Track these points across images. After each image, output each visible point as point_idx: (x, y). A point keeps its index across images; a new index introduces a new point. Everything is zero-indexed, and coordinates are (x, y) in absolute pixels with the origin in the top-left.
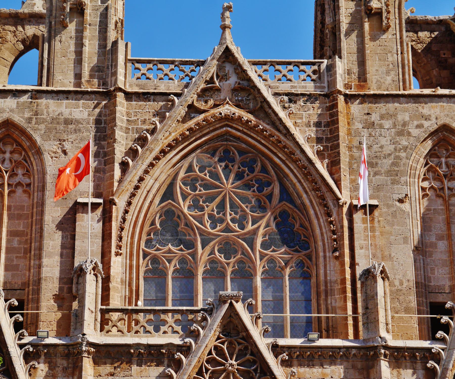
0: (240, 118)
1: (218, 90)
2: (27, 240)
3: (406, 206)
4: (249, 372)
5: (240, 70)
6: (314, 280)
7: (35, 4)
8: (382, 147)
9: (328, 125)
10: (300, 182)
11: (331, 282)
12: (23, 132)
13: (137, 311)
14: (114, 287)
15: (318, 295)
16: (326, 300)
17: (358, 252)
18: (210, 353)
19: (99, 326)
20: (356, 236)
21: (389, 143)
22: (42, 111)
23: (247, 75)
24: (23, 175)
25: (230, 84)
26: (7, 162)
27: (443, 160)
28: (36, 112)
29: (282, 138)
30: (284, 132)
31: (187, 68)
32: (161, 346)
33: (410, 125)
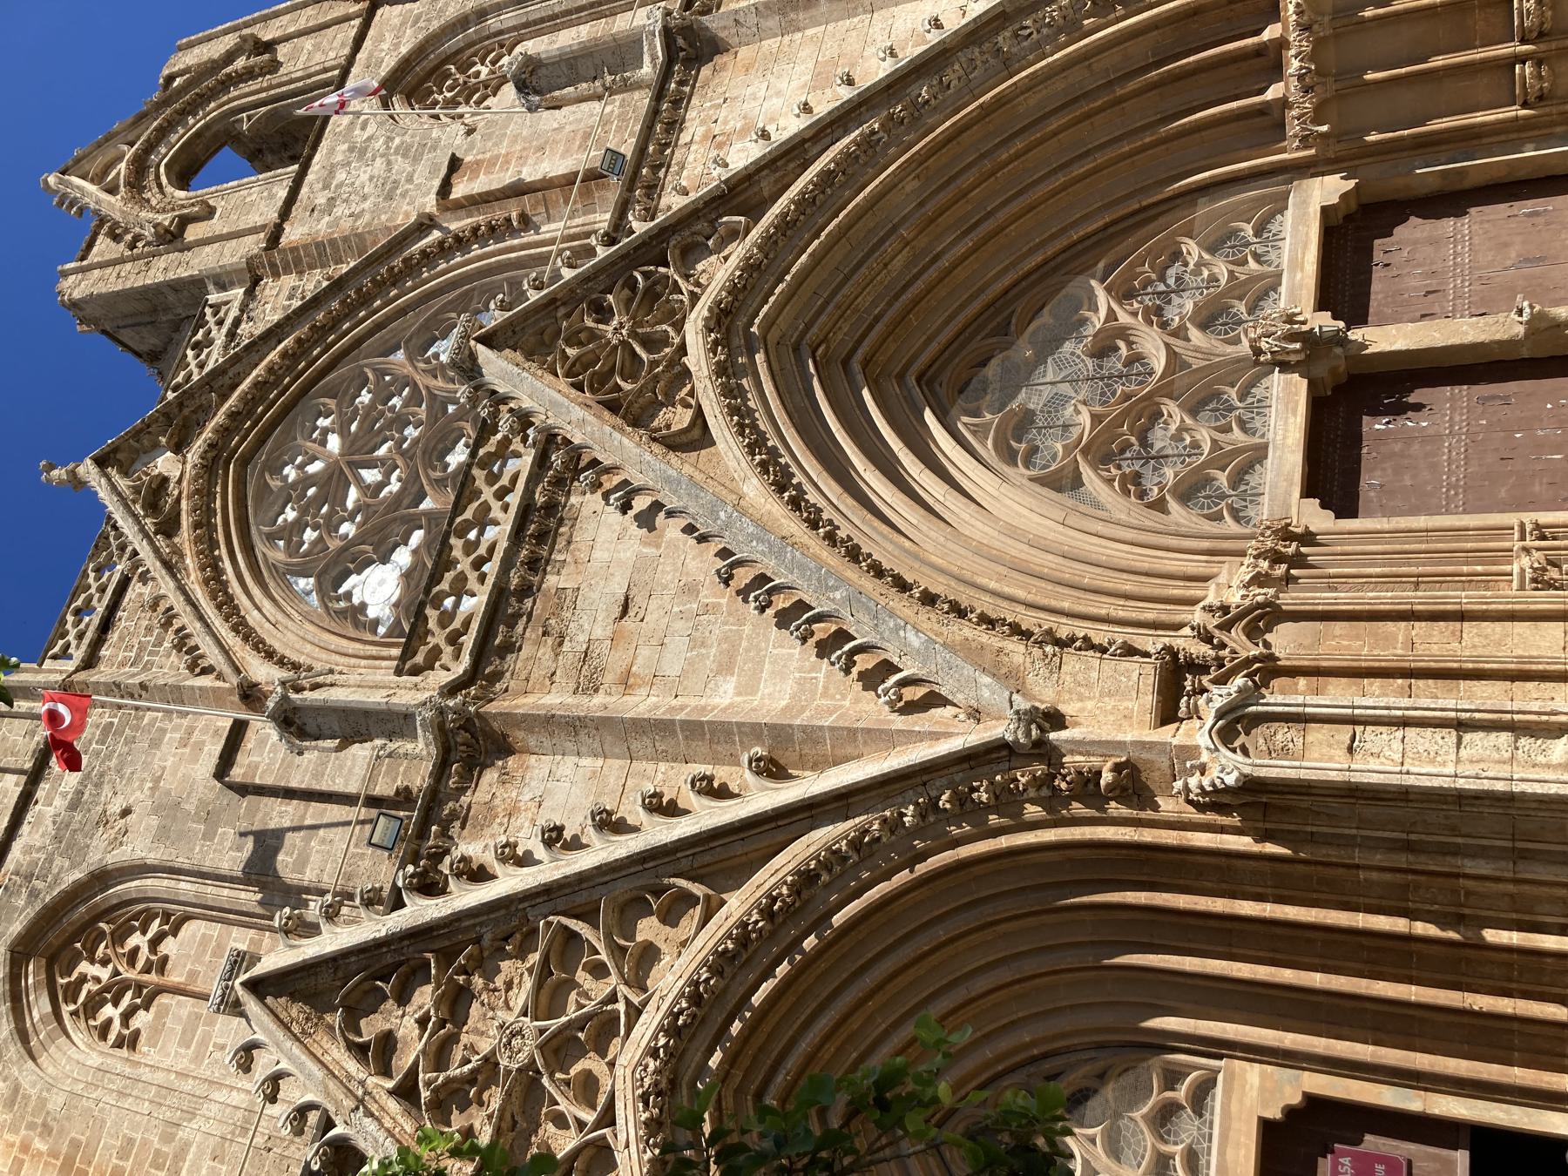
8: (371, 179)
28: (26, 878)
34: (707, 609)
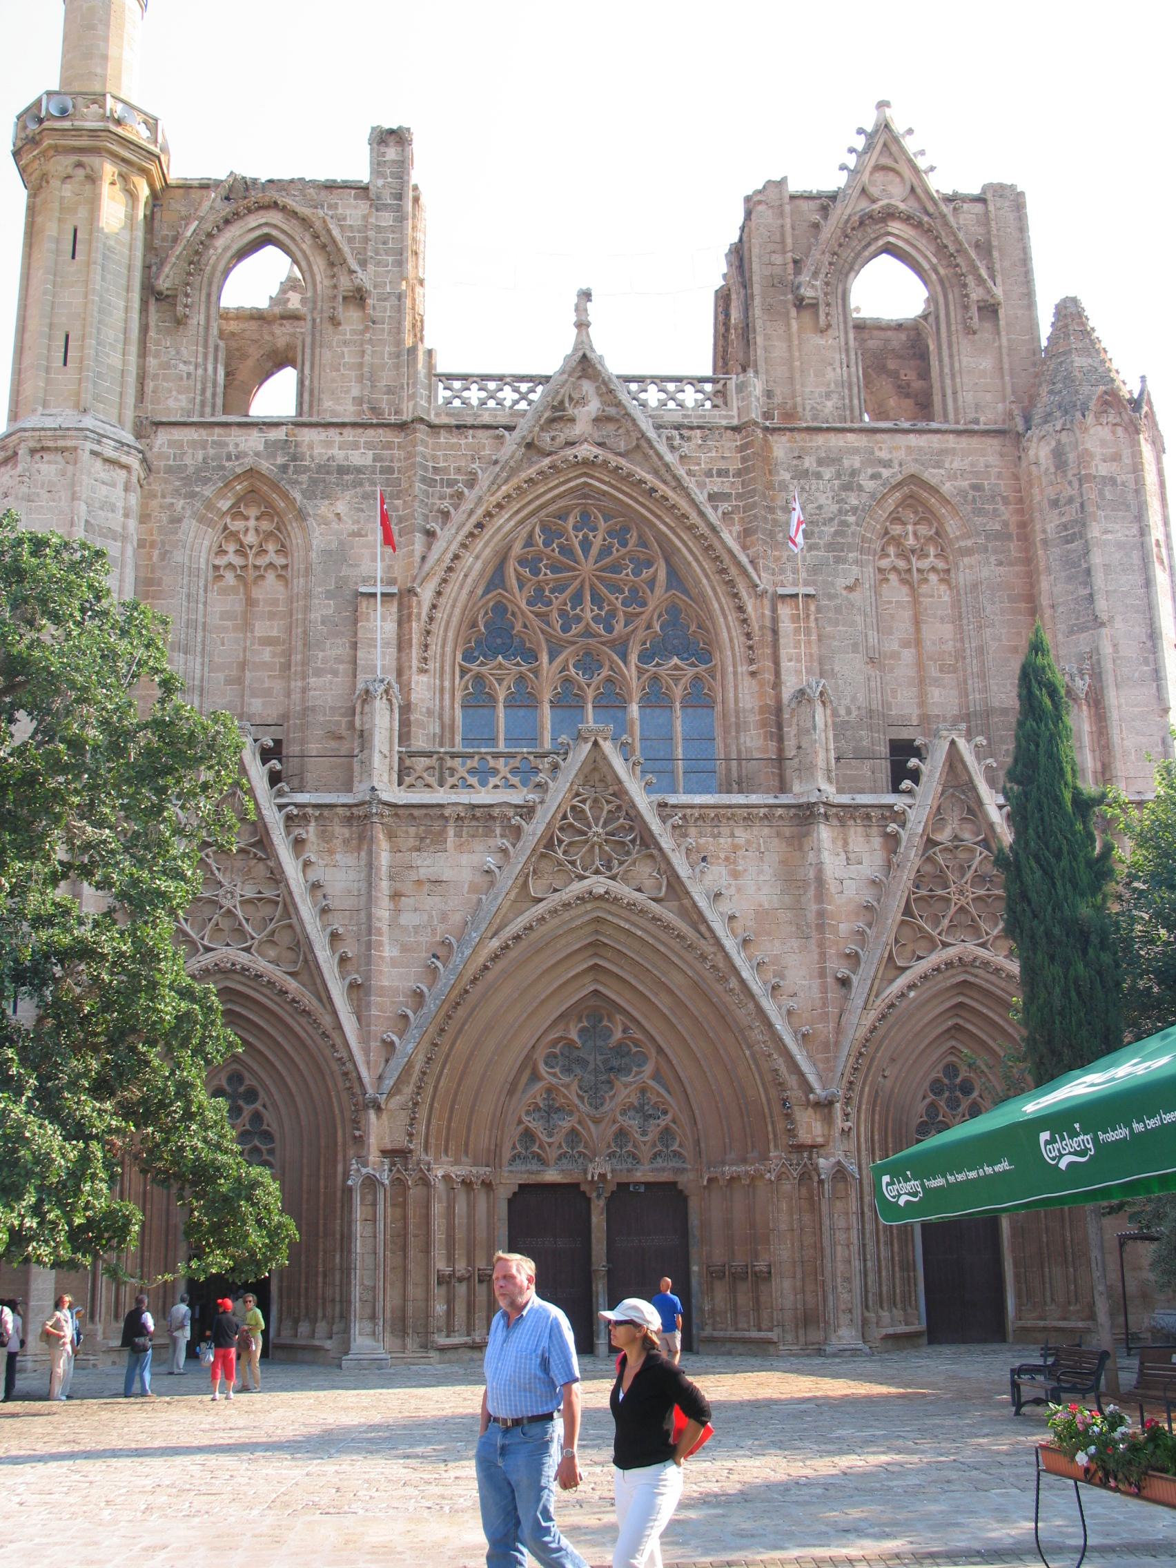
0: (606, 462)
1: (572, 420)
2: (283, 651)
3: (856, 596)
4: (623, 843)
5: (604, 390)
6: (719, 708)
7: (288, 300)
8: (820, 507)
9: (738, 473)
10: (697, 560)
11: (744, 710)
12: (275, 486)
13: (454, 756)
14: (417, 720)
15: (726, 730)
16: (737, 738)
17: (785, 665)
18: (565, 817)
19: (396, 776)
20: (782, 641)
21: (829, 502)
22: (303, 454)
23: (616, 397)
24: (277, 552)
25: (589, 413)
26: (251, 533)
27: (910, 528)
28: (294, 455)
29: (670, 493)
30: (674, 484)
31: (524, 387)
32: (491, 806)
33: (862, 476)
34: (434, 931)
